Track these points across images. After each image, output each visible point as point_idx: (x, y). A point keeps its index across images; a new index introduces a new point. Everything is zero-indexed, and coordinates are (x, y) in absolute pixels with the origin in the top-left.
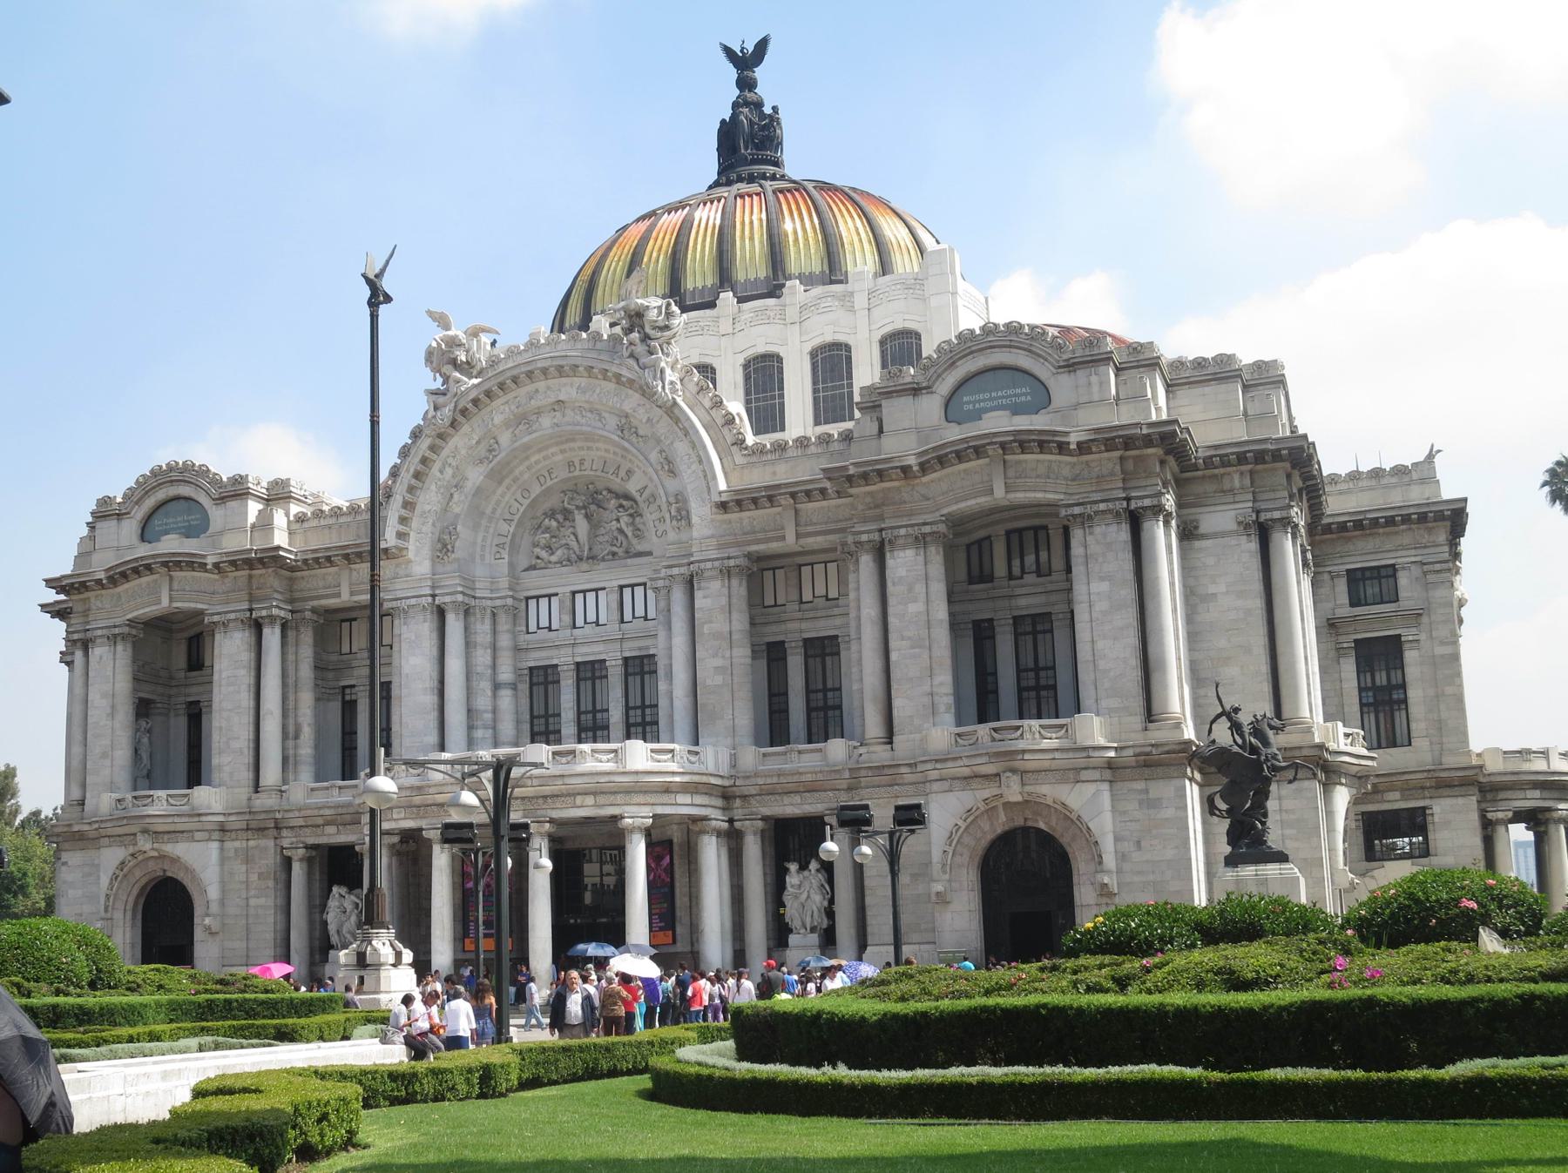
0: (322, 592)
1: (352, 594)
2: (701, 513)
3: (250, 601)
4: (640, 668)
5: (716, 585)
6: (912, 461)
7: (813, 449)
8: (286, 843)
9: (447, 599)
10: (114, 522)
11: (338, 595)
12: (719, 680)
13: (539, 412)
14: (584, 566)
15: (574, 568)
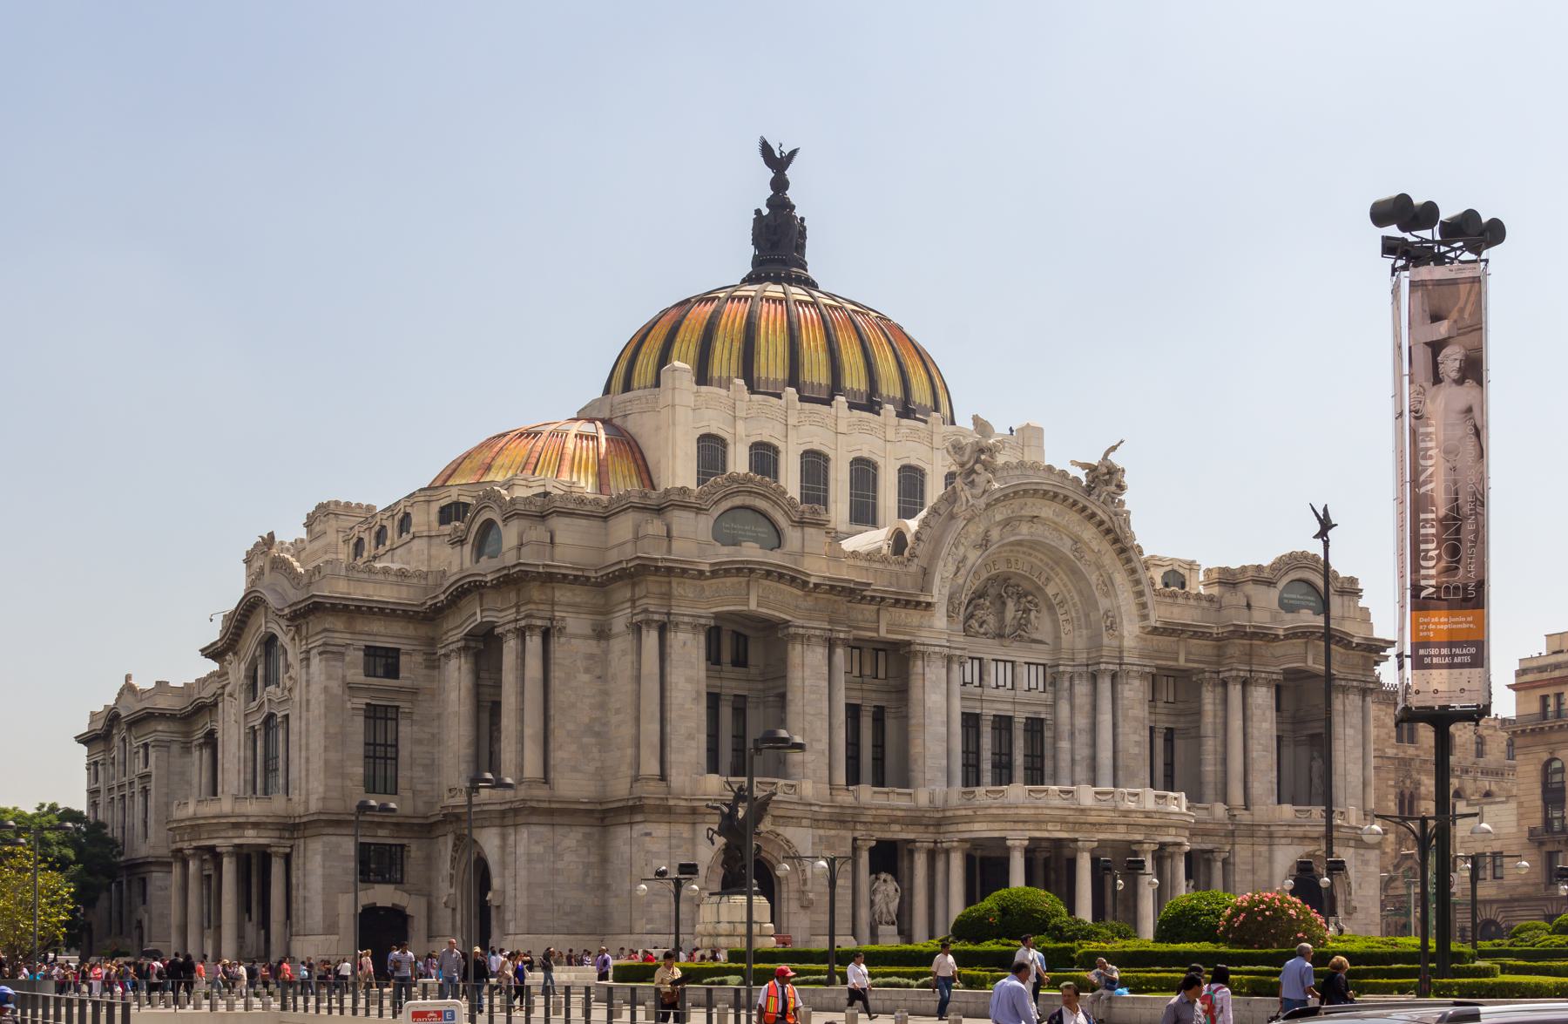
0: (862, 624)
1: (888, 632)
2: (1131, 631)
3: (831, 622)
4: (1035, 727)
5: (1137, 683)
6: (1281, 632)
7: (1192, 602)
8: (857, 834)
9: (958, 652)
10: (692, 515)
11: (877, 630)
12: (1136, 750)
13: (1020, 519)
14: (1007, 642)
15: (997, 641)
